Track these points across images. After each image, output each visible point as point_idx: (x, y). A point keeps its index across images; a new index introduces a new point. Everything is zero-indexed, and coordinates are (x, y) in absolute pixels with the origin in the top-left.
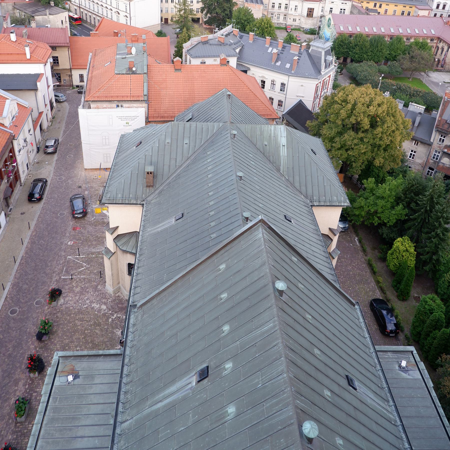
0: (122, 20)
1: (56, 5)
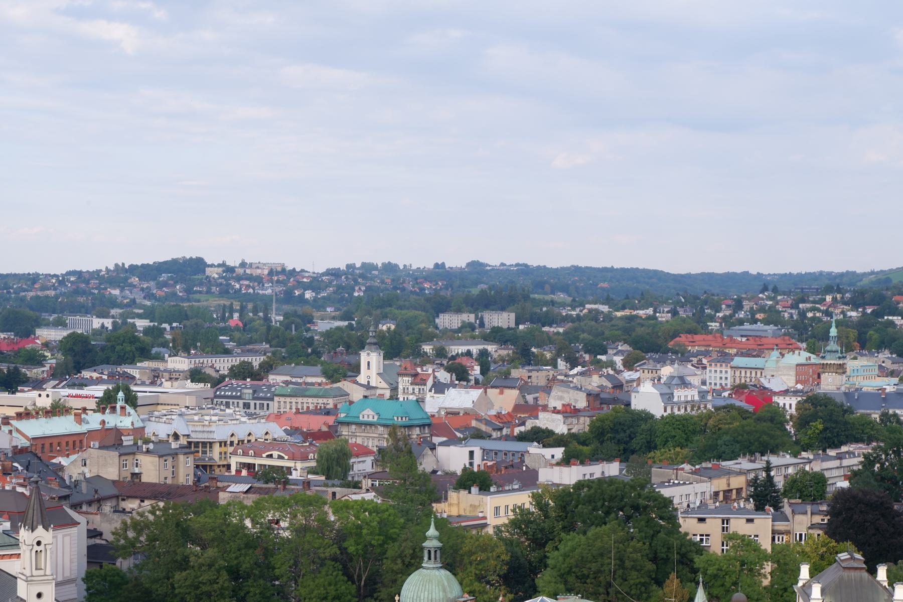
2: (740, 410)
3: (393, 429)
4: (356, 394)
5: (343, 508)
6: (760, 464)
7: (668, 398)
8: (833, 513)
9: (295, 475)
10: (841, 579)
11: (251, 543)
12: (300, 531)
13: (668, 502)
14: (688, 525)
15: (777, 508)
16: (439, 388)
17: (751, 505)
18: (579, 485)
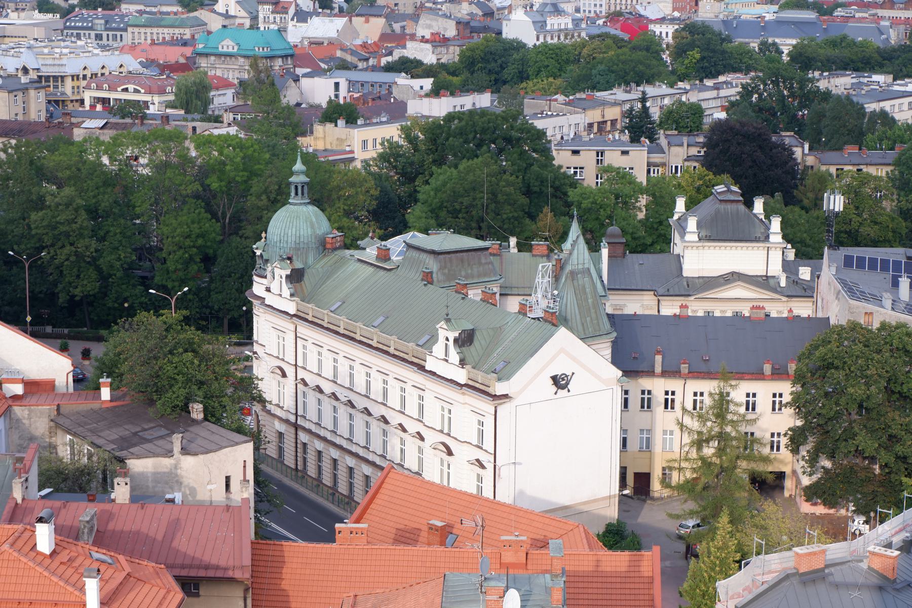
0: (463, 479)
1: (210, 415)
2: (616, 40)
3: (254, 60)
4: (215, 23)
5: (205, 143)
6: (635, 94)
7: (540, 26)
8: (710, 145)
9: (152, 110)
10: (717, 212)
11: (109, 181)
12: (160, 167)
13: (542, 134)
14: (562, 158)
15: (652, 139)
16: (302, 16)
17: (626, 137)
18: (450, 117)
